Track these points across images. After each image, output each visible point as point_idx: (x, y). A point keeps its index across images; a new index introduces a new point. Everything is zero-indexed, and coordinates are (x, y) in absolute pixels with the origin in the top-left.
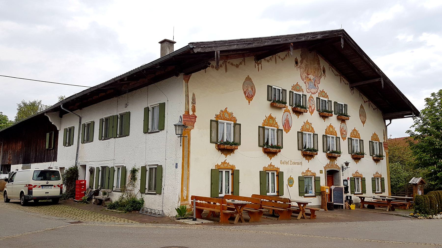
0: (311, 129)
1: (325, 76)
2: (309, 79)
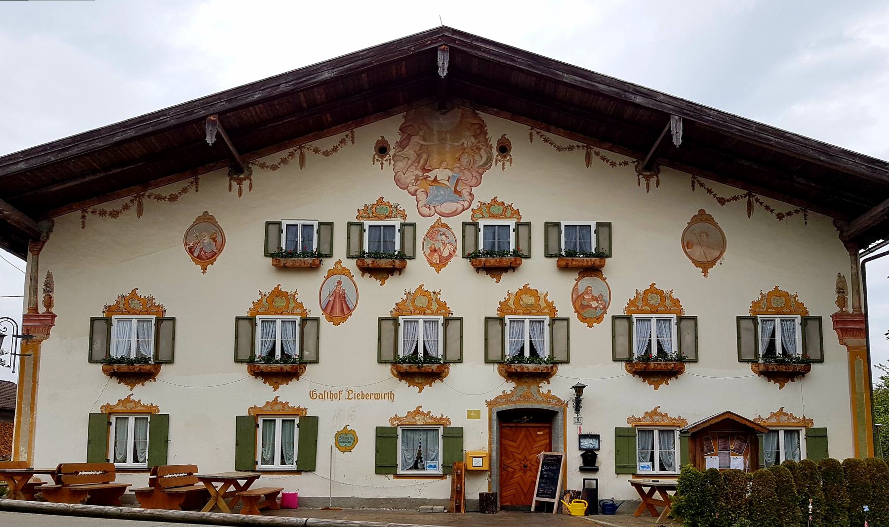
0: (435, 307)
1: (511, 161)
2: (430, 183)
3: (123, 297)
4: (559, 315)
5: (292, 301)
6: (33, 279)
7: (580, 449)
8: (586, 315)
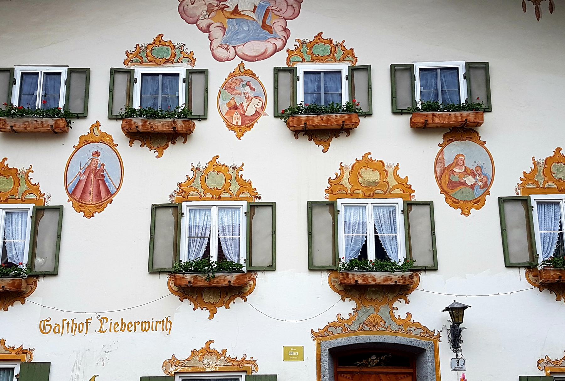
0: (235, 188)
2: (228, 15)
4: (417, 197)
5: (23, 182)
8: (458, 197)
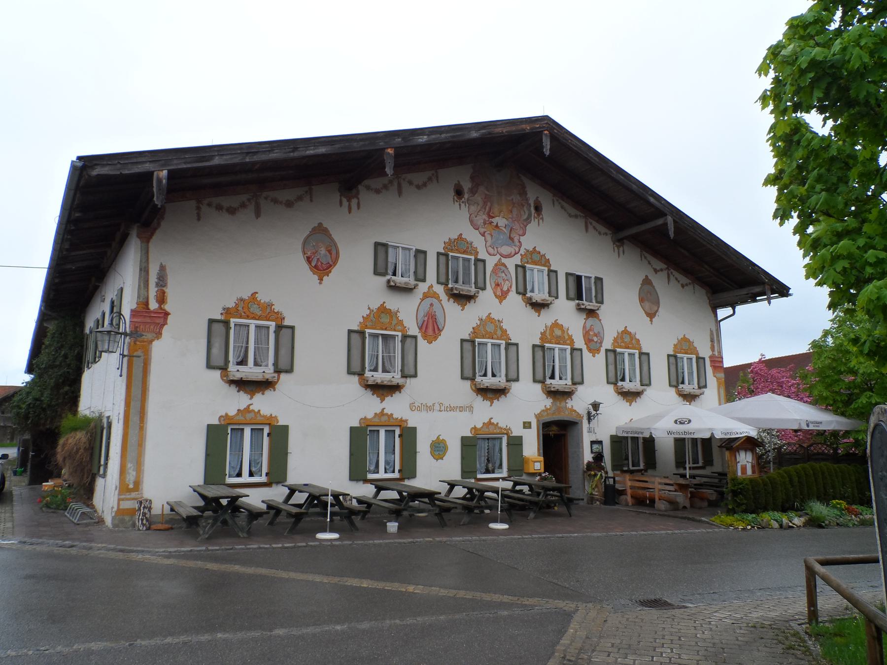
0: (499, 333)
1: (542, 219)
2: (493, 227)
3: (242, 300)
5: (394, 318)
6: (143, 269)
7: (592, 452)
8: (592, 347)
